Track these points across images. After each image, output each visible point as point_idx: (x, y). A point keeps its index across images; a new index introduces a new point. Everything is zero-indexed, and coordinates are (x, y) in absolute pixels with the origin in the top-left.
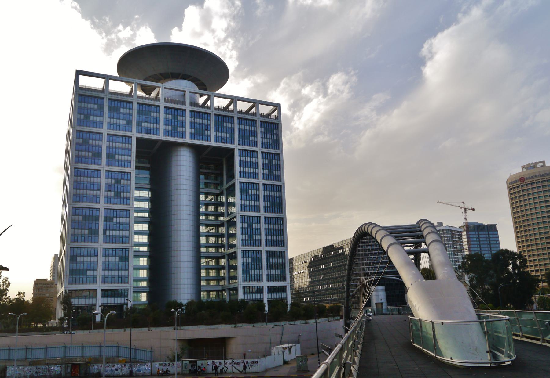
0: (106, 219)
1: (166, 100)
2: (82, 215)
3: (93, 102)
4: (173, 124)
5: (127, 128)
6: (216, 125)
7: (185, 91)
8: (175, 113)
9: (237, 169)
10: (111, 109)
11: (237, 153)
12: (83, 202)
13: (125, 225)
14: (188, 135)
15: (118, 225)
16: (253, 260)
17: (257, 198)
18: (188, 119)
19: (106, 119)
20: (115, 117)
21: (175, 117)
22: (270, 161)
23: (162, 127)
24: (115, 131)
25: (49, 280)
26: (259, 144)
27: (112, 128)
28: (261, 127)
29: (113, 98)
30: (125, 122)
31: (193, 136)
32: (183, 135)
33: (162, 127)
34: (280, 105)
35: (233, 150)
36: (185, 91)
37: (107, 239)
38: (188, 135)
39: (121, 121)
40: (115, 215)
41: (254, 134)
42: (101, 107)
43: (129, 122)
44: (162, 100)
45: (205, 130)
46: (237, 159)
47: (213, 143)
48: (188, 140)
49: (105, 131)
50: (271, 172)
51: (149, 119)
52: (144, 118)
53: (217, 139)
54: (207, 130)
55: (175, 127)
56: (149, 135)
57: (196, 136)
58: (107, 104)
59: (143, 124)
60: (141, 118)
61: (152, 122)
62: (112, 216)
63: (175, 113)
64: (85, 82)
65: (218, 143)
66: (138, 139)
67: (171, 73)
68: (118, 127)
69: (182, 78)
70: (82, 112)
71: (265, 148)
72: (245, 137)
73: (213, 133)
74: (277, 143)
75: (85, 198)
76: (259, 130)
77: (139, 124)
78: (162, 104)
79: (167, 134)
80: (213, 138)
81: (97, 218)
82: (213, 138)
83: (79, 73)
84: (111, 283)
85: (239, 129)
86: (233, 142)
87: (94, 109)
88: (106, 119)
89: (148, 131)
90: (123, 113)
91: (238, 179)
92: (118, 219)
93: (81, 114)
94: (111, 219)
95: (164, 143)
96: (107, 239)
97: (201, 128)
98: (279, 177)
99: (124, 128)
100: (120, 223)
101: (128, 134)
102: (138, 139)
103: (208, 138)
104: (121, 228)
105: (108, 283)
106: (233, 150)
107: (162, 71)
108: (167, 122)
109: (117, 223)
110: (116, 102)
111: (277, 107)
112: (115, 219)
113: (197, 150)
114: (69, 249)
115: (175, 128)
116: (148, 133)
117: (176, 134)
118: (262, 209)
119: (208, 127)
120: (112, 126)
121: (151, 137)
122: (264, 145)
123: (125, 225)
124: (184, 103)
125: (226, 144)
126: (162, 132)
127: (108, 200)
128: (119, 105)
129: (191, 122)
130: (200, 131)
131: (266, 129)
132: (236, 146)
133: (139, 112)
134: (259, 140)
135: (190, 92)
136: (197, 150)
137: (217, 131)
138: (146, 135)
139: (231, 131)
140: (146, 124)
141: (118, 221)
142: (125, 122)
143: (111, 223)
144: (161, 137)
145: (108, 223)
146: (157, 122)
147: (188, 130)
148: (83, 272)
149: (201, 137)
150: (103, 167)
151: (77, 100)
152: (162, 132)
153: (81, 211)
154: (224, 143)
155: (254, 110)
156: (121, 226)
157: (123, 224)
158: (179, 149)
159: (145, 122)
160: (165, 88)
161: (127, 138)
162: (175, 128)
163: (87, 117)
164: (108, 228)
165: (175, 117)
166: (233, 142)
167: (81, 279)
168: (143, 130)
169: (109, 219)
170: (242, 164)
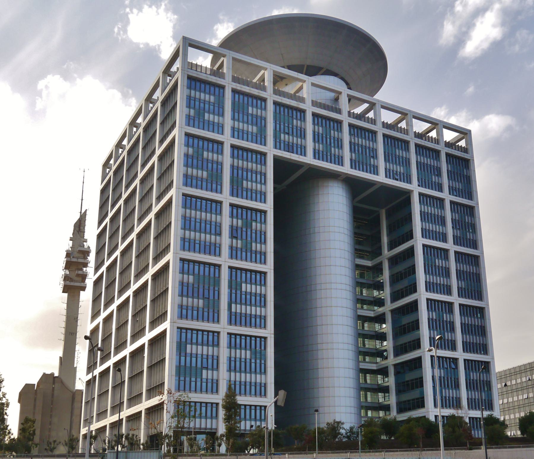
1: (315, 104)
7: (340, 93)
8: (327, 124)
19: (228, 121)
25: (56, 374)
32: (340, 161)
36: (340, 93)
37: (234, 318)
43: (262, 130)
44: (309, 102)
46: (416, 208)
47: (381, 178)
48: (346, 169)
49: (228, 139)
55: (328, 146)
72: (429, 174)
78: (310, 109)
89: (289, 148)
96: (234, 318)
98: (475, 244)
111: (465, 133)
113: (354, 186)
114: (176, 329)
121: (294, 157)
127: (234, 253)
130: (364, 158)
132: (415, 188)
136: (354, 186)
139: (407, 163)
144: (309, 159)
146: (302, 134)
148: (197, 372)
150: (226, 197)
154: (397, 180)
155: (433, 134)
160: (313, 85)
163: (200, 113)
170: (424, 216)
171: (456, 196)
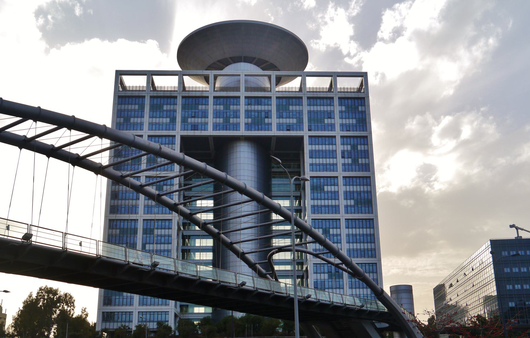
0: (145, 232)
2: (120, 228)
3: (130, 102)
4: (225, 116)
5: (171, 126)
6: (278, 110)
9: (308, 160)
10: (153, 108)
11: (306, 141)
12: (121, 213)
13: (167, 238)
14: (242, 126)
15: (159, 238)
16: (330, 277)
17: (335, 195)
18: (242, 107)
20: (158, 116)
21: (227, 107)
22: (354, 147)
23: (211, 120)
24: (157, 131)
26: (338, 127)
27: (154, 128)
28: (341, 105)
29: (155, 95)
30: (168, 120)
31: (248, 127)
32: (236, 126)
33: (211, 120)
34: (366, 73)
35: (301, 138)
38: (242, 126)
39: (165, 119)
40: (156, 226)
41: (330, 115)
42: (142, 108)
43: (173, 120)
45: (266, 117)
46: (307, 148)
47: (274, 132)
48: (242, 132)
50: (355, 161)
51: (197, 114)
52: (190, 113)
53: (280, 127)
54: (267, 117)
55: (226, 118)
56: (196, 132)
57: (253, 126)
58: (149, 103)
59: (189, 120)
60: (187, 113)
61: (200, 116)
62: (152, 227)
63: (226, 101)
64: (130, 82)
65: (281, 132)
66: (183, 138)
67: (231, 58)
68: (161, 127)
69: (245, 61)
70: (122, 115)
71: (347, 131)
72: (316, 120)
73: (274, 120)
74: (363, 122)
75: (123, 209)
76: (337, 108)
77: (184, 120)
79: (218, 128)
80: (274, 127)
81: (135, 231)
82: (274, 127)
83: (119, 74)
84: (150, 305)
85: (309, 112)
86: (301, 129)
87: (135, 110)
88: (146, 120)
89: (195, 127)
90: (167, 111)
91: (308, 173)
92: (159, 230)
93: (121, 117)
94: (151, 231)
95: (217, 139)
97: (260, 116)
98: (369, 167)
99: (168, 126)
100: (161, 236)
101: (171, 133)
102: (183, 138)
103: (268, 126)
104: (163, 241)
105: (147, 305)
106: (301, 138)
107: (220, 58)
108: (217, 114)
109: (158, 236)
110: (159, 100)
112: (156, 231)
115: (227, 120)
116: (195, 130)
117: (228, 126)
118: (342, 209)
119: (268, 114)
120: (154, 126)
121: (197, 133)
122: (343, 127)
123: (167, 238)
124: (237, 89)
125: (291, 132)
126: (210, 126)
128: (162, 102)
129: (247, 111)
130: (258, 120)
131: (347, 107)
132: (305, 133)
133: (184, 107)
134: (337, 121)
135: (245, 75)
137: (280, 116)
138: (193, 131)
139: (299, 116)
140: (193, 119)
141: (159, 233)
142: (168, 120)
143: (152, 236)
144: (210, 132)
145: (148, 236)
146: (205, 115)
147: (243, 120)
149: (260, 126)
151: (117, 102)
152: (210, 126)
153: (118, 223)
156: (163, 238)
157: (165, 236)
158: (238, 144)
159: (192, 117)
161: (171, 138)
162: (227, 120)
163: (127, 120)
164: (148, 241)
165: (227, 107)
166: (301, 129)
167: (117, 300)
168: (190, 126)
169: (148, 231)
171: (349, 131)
